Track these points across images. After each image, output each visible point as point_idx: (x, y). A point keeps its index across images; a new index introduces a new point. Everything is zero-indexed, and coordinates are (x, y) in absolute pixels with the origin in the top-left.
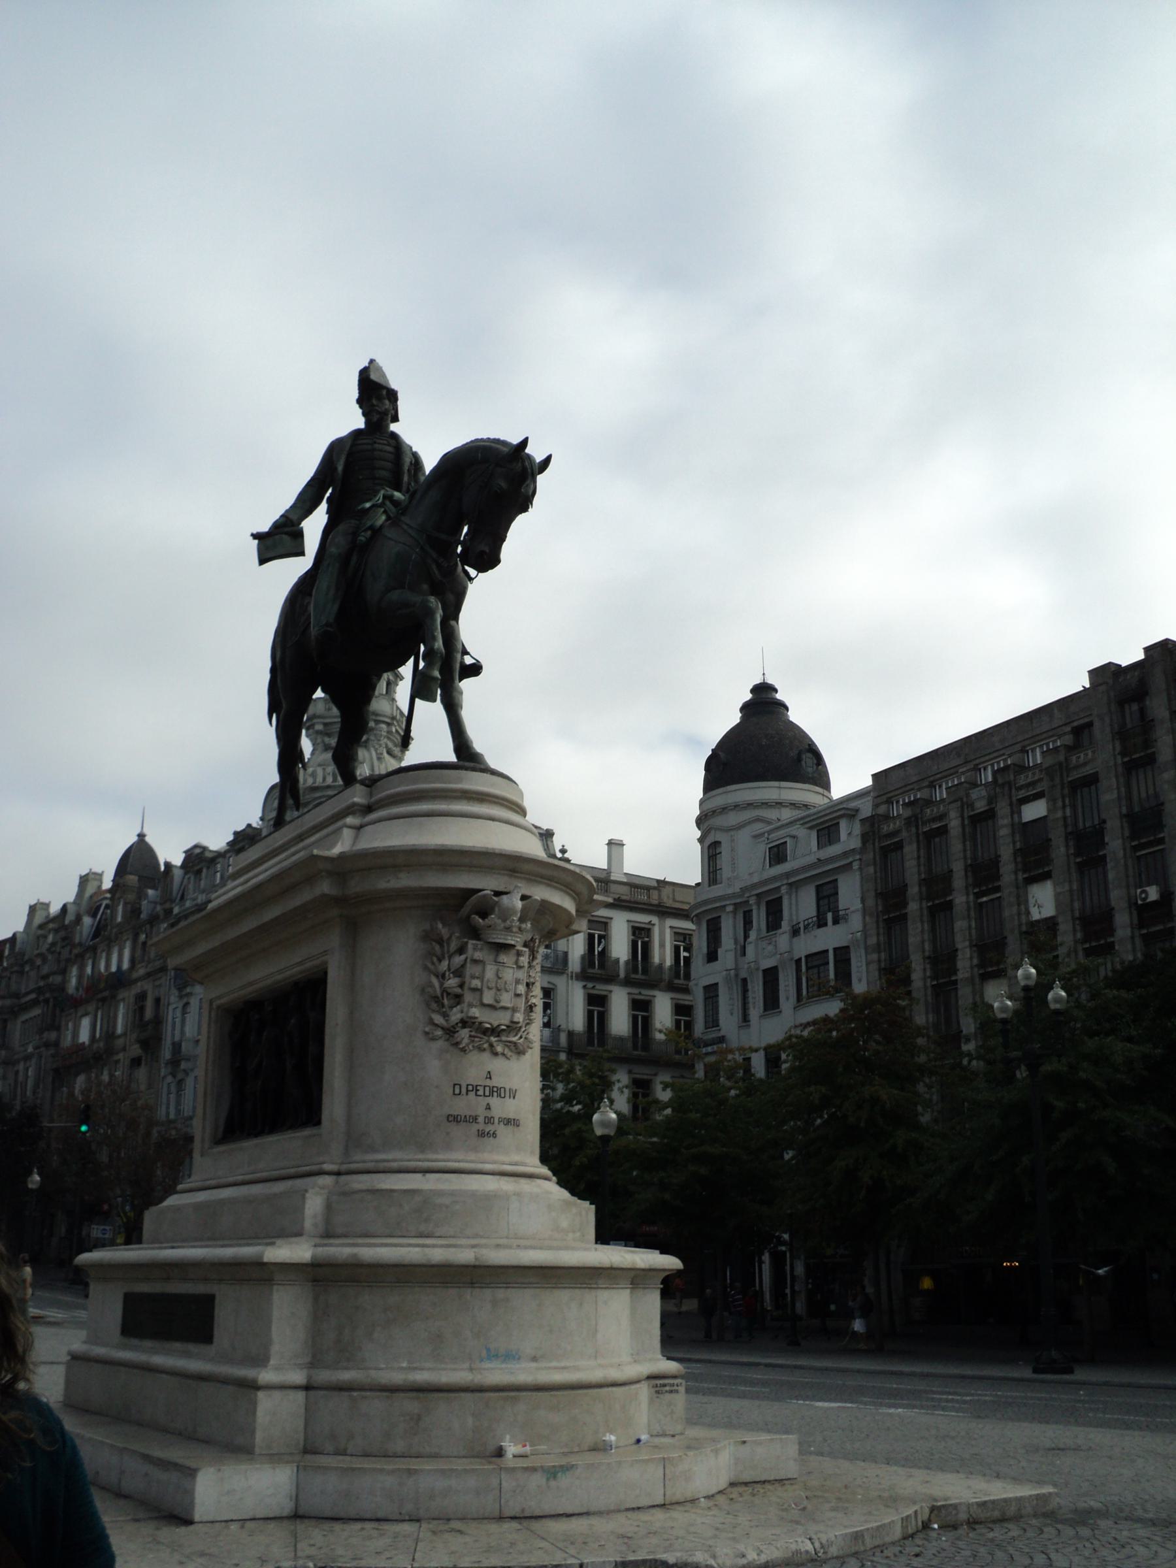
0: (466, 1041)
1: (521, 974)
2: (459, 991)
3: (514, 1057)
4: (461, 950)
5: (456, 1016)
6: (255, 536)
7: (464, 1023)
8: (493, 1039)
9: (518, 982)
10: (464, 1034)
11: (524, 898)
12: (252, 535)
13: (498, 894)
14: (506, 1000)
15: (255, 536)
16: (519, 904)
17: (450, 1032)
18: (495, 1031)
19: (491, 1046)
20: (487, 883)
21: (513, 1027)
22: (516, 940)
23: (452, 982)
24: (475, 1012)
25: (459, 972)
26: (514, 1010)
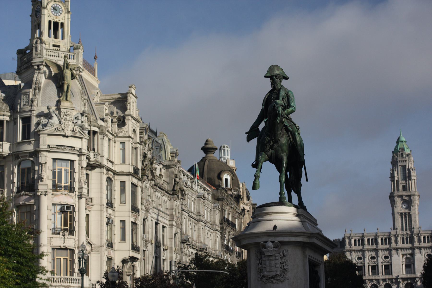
0: (265, 281)
1: (277, 262)
2: (262, 268)
3: (280, 283)
4: (261, 257)
5: (262, 275)
6: (246, 133)
7: (264, 276)
8: (272, 280)
9: (276, 264)
10: (264, 279)
11: (272, 242)
12: (246, 133)
13: (266, 242)
14: (273, 269)
15: (246, 133)
16: (270, 244)
17: (262, 279)
18: (272, 277)
19: (272, 281)
20: (261, 240)
21: (277, 276)
22: (274, 253)
23: (260, 266)
24: (266, 273)
25: (261, 264)
26: (276, 271)
